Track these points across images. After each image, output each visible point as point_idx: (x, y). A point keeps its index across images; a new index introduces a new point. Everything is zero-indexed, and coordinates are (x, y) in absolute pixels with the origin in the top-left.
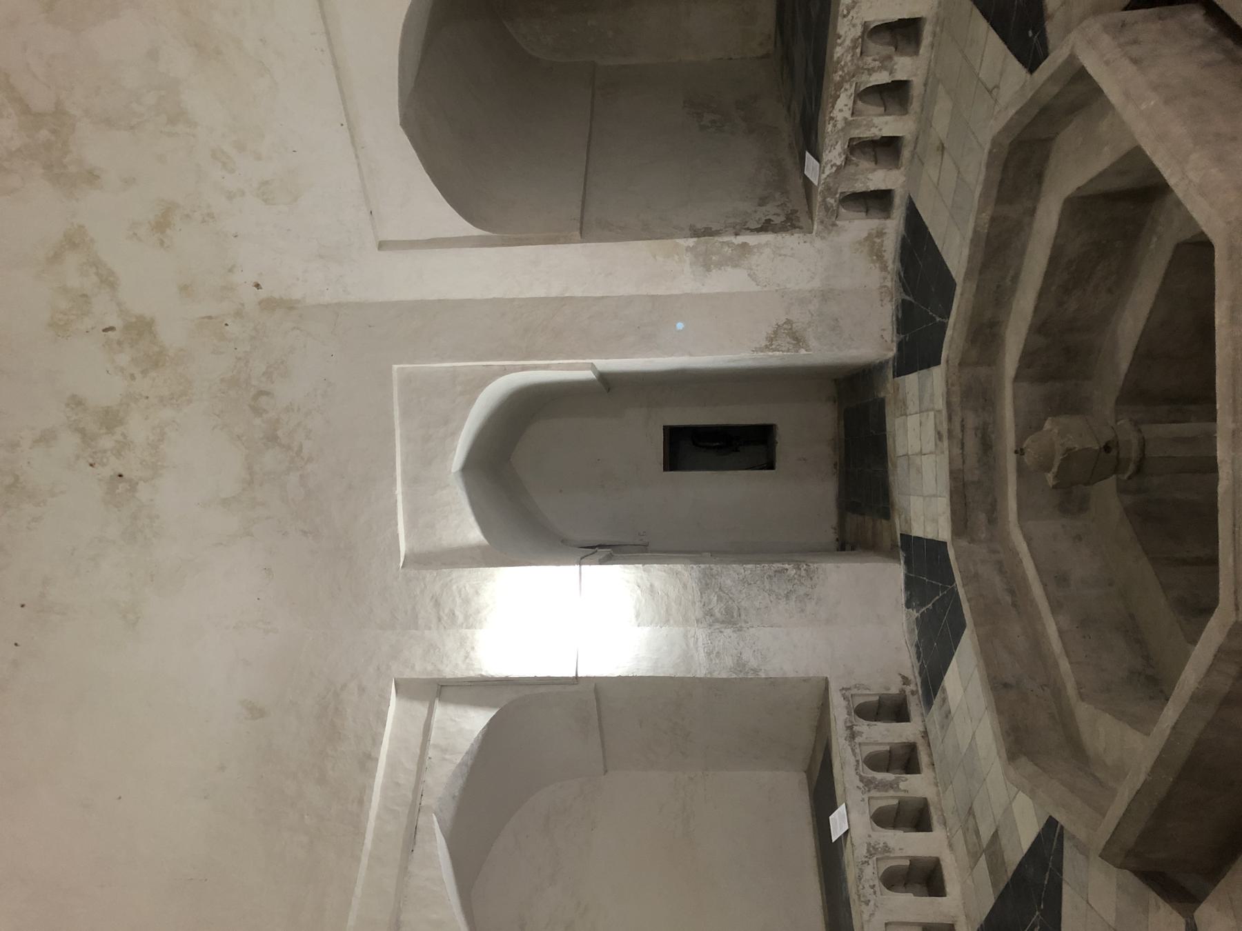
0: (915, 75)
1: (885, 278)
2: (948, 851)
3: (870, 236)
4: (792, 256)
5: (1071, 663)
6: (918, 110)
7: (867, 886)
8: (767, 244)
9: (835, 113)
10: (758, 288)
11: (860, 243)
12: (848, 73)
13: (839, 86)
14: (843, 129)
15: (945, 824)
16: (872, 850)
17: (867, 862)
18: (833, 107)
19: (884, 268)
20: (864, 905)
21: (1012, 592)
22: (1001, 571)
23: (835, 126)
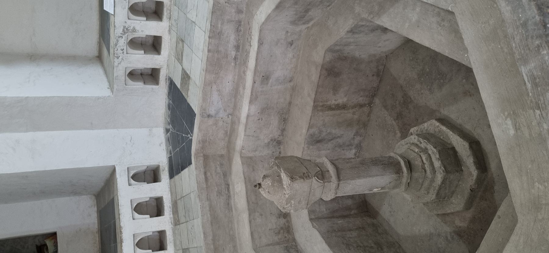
2: (167, 33)
5: (245, 135)
7: (119, 49)
15: (170, 18)
16: (126, 30)
17: (122, 37)
20: (116, 59)
21: (237, 48)
22: (238, 30)
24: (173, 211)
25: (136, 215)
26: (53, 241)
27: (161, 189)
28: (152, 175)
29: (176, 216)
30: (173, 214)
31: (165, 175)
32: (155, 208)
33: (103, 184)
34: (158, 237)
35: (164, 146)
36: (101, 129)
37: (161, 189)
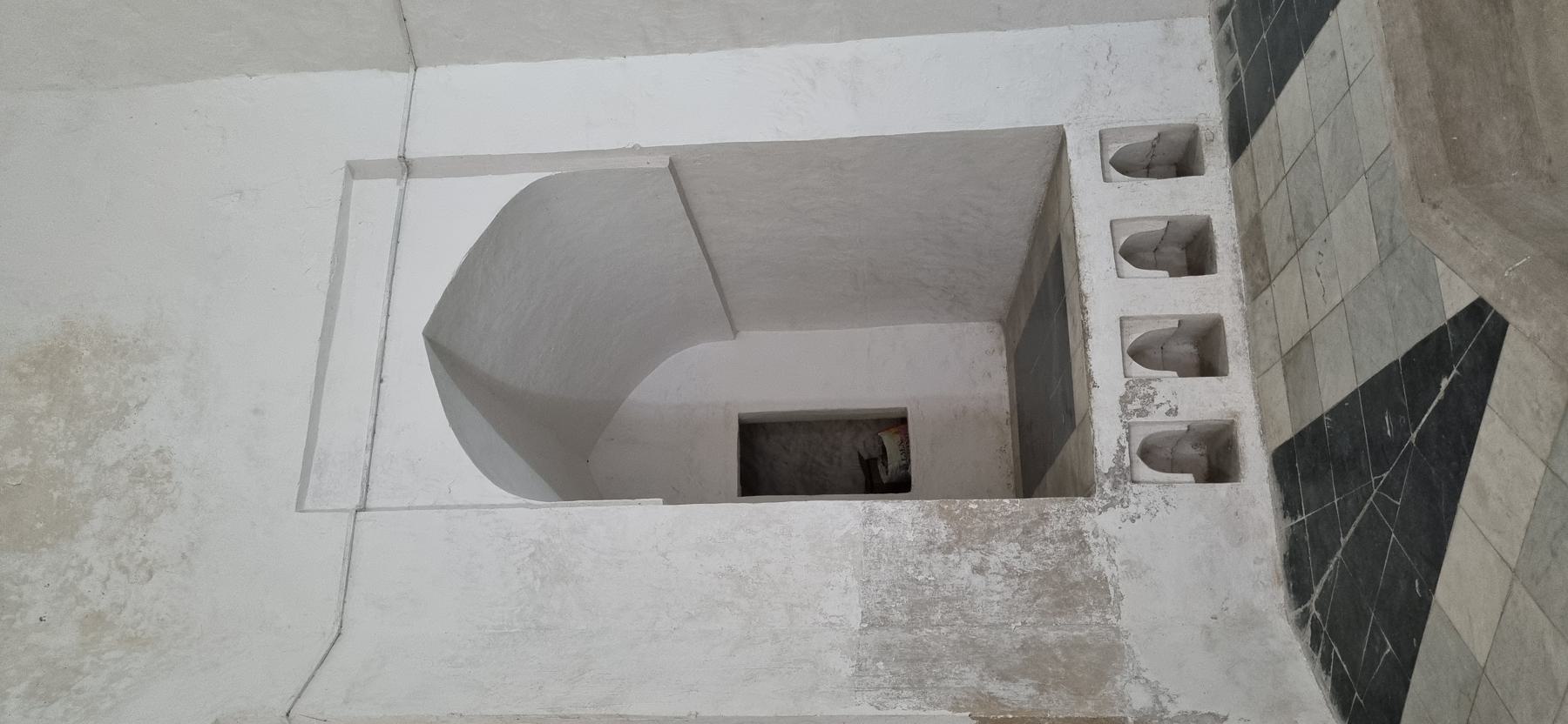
24: (1244, 251)
25: (1127, 267)
26: (898, 438)
27: (1207, 196)
28: (1176, 157)
29: (1259, 268)
30: (1246, 267)
31: (1216, 157)
32: (1191, 252)
33: (1023, 245)
34: (1195, 360)
35: (1211, 71)
36: (1023, 28)
37: (1207, 196)
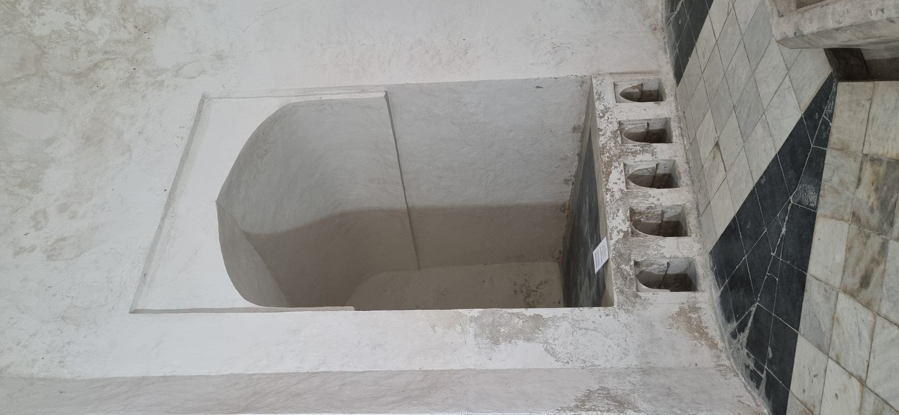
0: (676, 156)
1: (719, 357)
3: (681, 312)
4: (595, 330)
6: (689, 183)
8: (564, 317)
9: (610, 185)
10: (558, 365)
11: (672, 317)
12: (615, 155)
13: (609, 164)
14: (621, 199)
18: (607, 181)
19: (713, 345)
23: (612, 196)
